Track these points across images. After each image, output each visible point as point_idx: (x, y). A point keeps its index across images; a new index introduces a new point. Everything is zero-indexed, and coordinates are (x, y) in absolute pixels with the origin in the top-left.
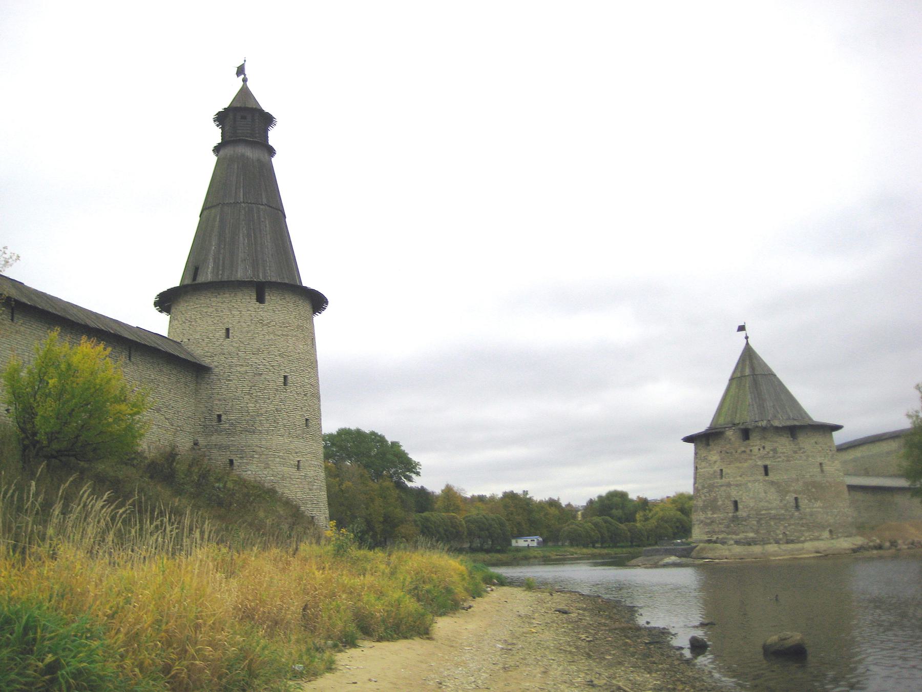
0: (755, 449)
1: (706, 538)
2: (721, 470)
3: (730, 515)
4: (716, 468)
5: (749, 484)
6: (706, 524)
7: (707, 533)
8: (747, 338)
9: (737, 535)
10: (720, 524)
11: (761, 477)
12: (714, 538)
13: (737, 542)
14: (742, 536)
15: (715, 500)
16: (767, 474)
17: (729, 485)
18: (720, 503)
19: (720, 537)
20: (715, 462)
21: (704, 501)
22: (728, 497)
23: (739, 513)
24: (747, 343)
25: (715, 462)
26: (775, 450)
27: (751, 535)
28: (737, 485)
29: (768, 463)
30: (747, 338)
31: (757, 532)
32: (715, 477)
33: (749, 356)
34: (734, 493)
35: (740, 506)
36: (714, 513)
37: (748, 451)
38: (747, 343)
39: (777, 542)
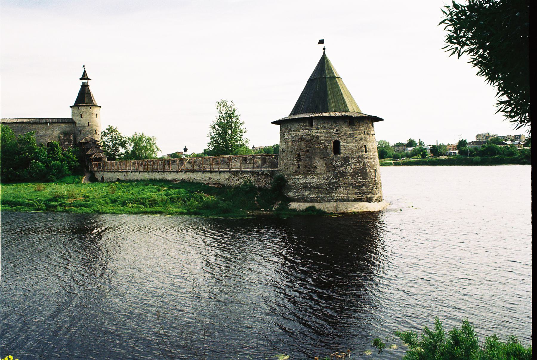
1: (356, 197)
2: (365, 146)
6: (355, 187)
7: (356, 194)
8: (324, 49)
15: (364, 169)
18: (367, 171)
20: (361, 139)
21: (354, 169)
23: (376, 179)
24: (324, 53)
25: (361, 139)
30: (324, 49)
32: (362, 151)
33: (324, 64)
36: (364, 178)
38: (324, 53)
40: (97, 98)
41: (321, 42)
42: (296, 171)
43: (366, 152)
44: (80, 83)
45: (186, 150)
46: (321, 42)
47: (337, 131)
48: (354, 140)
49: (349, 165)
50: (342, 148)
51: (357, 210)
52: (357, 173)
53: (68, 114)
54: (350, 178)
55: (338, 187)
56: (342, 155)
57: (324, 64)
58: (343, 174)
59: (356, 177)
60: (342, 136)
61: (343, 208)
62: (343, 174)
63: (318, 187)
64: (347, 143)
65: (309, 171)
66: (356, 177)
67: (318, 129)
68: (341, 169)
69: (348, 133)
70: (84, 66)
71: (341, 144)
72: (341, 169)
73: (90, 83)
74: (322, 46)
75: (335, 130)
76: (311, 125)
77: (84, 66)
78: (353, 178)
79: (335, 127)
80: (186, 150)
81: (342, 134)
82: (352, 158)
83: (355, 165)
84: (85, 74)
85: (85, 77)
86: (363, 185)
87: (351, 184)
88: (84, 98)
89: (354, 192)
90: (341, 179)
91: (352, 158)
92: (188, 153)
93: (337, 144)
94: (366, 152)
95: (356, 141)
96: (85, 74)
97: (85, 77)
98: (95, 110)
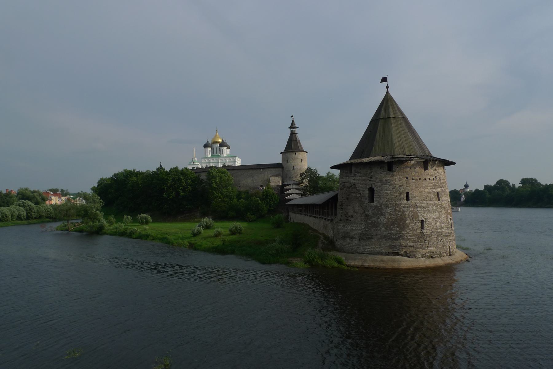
0: (432, 178)
1: (391, 251)
2: (407, 194)
3: (419, 231)
4: (403, 191)
5: (430, 207)
7: (391, 247)
8: (387, 87)
9: (424, 249)
10: (409, 239)
11: (437, 202)
12: (402, 252)
13: (423, 256)
14: (427, 250)
16: (439, 200)
17: (416, 207)
18: (407, 222)
19: (408, 251)
20: (401, 186)
22: (416, 215)
23: (424, 231)
25: (400, 186)
26: (440, 180)
27: (433, 249)
28: (420, 207)
29: (439, 190)
30: (387, 87)
31: (436, 247)
34: (421, 214)
35: (426, 225)
37: (428, 179)
39: (447, 255)
40: (304, 143)
41: (384, 80)
42: (341, 220)
43: (408, 199)
44: (289, 131)
45: (466, 186)
46: (384, 80)
47: (371, 178)
48: (391, 187)
49: (382, 215)
50: (376, 196)
51: (372, 264)
52: (393, 224)
53: (278, 159)
54: (383, 229)
55: (370, 238)
56: (375, 204)
57: (388, 102)
58: (375, 225)
59: (390, 228)
60: (378, 182)
61: (370, 261)
62: (375, 225)
63: (352, 238)
64: (382, 190)
65: (347, 220)
66: (390, 228)
67: (355, 175)
68: (373, 219)
69: (384, 179)
70: (292, 116)
71: (375, 192)
72: (373, 219)
73: (297, 131)
74: (385, 84)
75: (370, 176)
76: (351, 172)
77: (292, 116)
78: (386, 228)
79: (371, 173)
80: (466, 186)
81: (377, 181)
82: (388, 207)
83: (390, 215)
84: (293, 123)
85: (293, 126)
86: (399, 238)
87: (385, 237)
88: (293, 146)
89: (388, 245)
90: (373, 229)
91: (388, 207)
92: (472, 188)
93: (372, 190)
94: (408, 199)
95: (394, 188)
96: (293, 123)
97: (293, 126)
98: (300, 155)
